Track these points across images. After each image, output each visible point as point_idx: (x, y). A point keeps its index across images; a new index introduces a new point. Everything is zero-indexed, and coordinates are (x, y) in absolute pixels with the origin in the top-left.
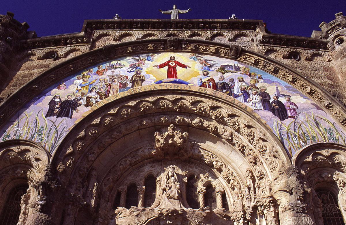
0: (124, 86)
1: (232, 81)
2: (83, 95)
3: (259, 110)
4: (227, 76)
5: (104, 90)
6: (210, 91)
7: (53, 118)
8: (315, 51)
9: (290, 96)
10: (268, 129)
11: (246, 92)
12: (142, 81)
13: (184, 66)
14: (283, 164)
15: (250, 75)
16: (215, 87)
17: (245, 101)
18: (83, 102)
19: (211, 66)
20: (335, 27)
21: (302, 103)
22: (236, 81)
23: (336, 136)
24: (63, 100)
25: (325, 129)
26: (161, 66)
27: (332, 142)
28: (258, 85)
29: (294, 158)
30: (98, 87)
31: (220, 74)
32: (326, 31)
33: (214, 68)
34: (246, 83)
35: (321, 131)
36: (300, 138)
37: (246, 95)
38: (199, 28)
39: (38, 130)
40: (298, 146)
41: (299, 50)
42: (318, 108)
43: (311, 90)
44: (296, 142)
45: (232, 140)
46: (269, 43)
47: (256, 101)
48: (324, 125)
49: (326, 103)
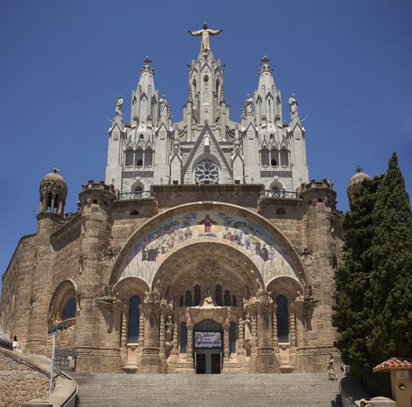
0: (181, 238)
2: (159, 245)
5: (170, 242)
6: (228, 242)
7: (146, 262)
8: (294, 207)
12: (191, 234)
13: (215, 223)
16: (231, 239)
18: (160, 250)
19: (230, 223)
24: (149, 249)
26: (201, 223)
30: (167, 239)
37: (248, 244)
39: (141, 270)
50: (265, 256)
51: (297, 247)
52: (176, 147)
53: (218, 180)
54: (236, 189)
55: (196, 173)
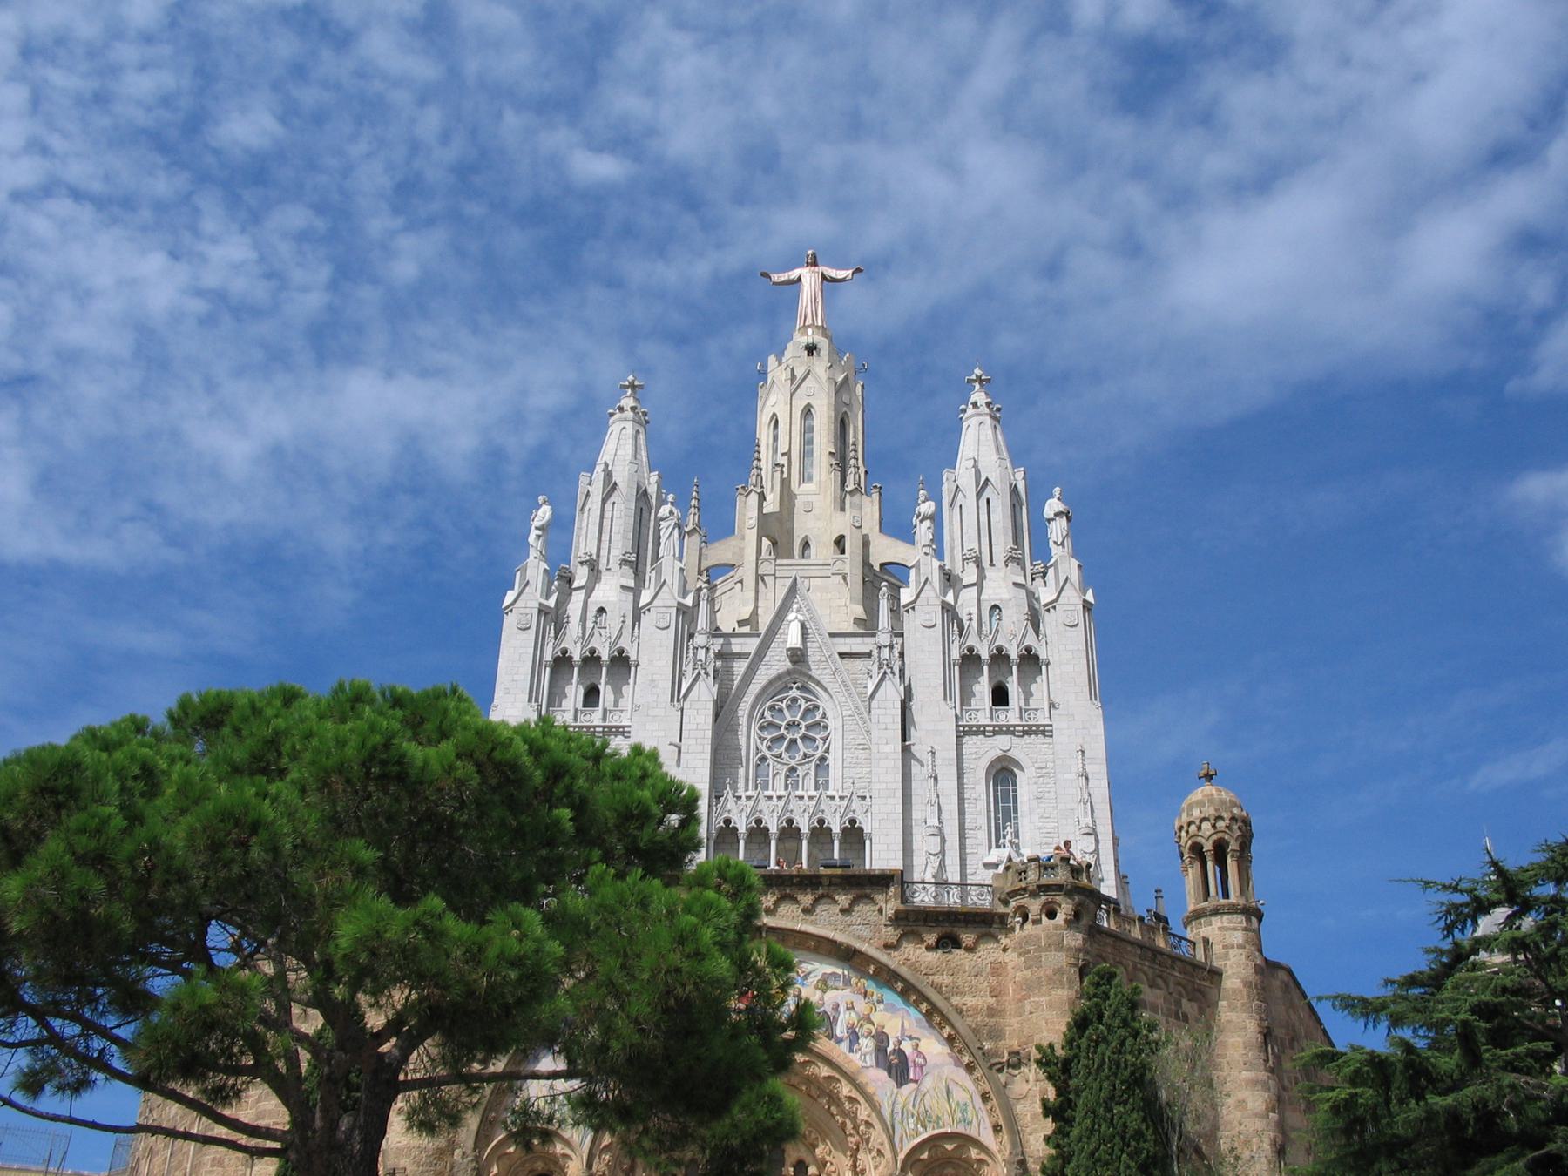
1: (836, 1008)
3: (867, 1068)
4: (830, 996)
8: (984, 930)
9: (919, 1039)
10: (875, 1107)
11: (854, 1032)
14: (888, 1162)
15: (865, 994)
17: (851, 1050)
20: (1018, 890)
21: (935, 1052)
22: (842, 1009)
23: (969, 1115)
25: (958, 1104)
27: (960, 1129)
28: (876, 1017)
29: (902, 1156)
31: (819, 993)
32: (1007, 891)
33: (810, 980)
34: (857, 1014)
35: (950, 1107)
36: (918, 1118)
37: (854, 1037)
38: (792, 884)
40: (912, 1132)
41: (955, 929)
42: (958, 1063)
43: (950, 1035)
44: (912, 1126)
45: (829, 1108)
46: (906, 919)
47: (868, 1049)
48: (959, 1095)
49: (966, 1059)
50: (899, 1068)
51: (987, 1045)
52: (701, 654)
53: (827, 750)
54: (826, 881)
55: (762, 728)
